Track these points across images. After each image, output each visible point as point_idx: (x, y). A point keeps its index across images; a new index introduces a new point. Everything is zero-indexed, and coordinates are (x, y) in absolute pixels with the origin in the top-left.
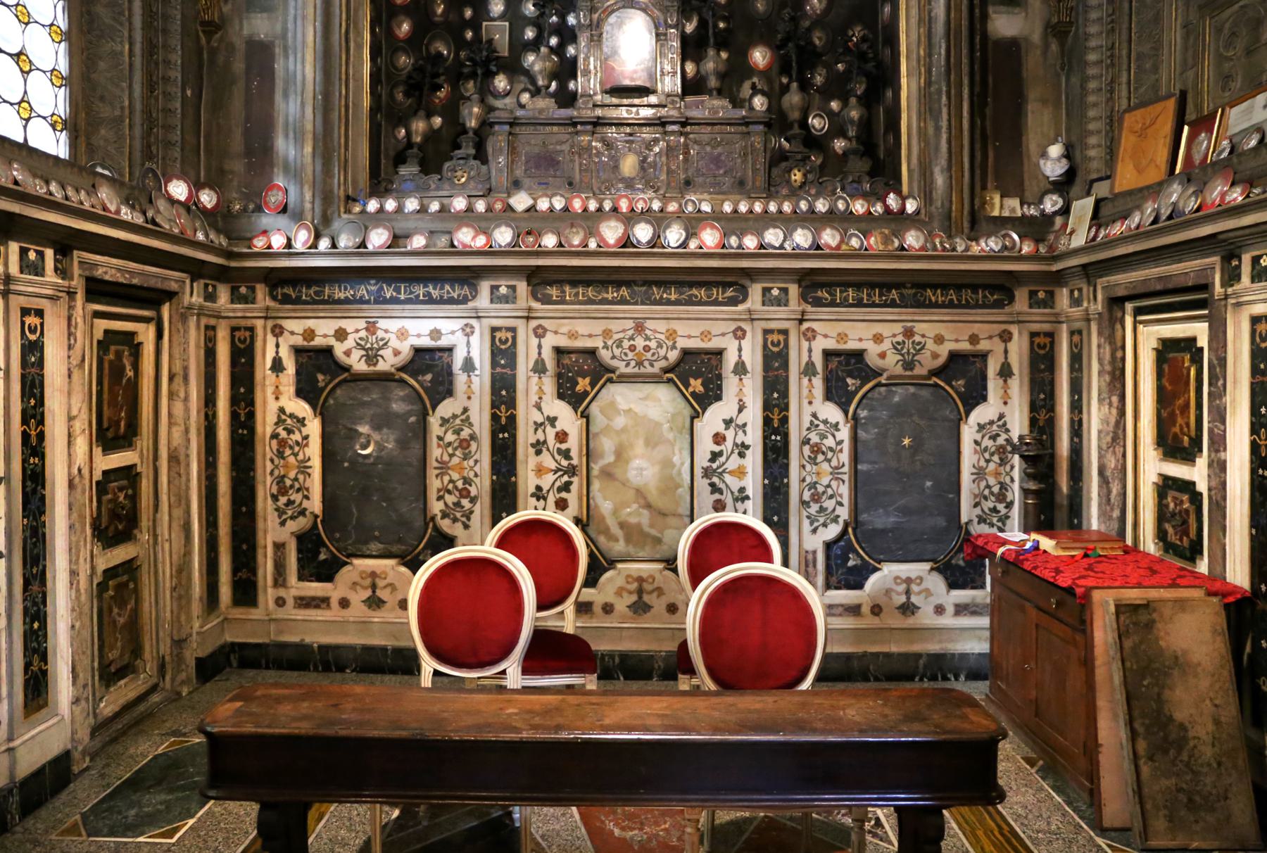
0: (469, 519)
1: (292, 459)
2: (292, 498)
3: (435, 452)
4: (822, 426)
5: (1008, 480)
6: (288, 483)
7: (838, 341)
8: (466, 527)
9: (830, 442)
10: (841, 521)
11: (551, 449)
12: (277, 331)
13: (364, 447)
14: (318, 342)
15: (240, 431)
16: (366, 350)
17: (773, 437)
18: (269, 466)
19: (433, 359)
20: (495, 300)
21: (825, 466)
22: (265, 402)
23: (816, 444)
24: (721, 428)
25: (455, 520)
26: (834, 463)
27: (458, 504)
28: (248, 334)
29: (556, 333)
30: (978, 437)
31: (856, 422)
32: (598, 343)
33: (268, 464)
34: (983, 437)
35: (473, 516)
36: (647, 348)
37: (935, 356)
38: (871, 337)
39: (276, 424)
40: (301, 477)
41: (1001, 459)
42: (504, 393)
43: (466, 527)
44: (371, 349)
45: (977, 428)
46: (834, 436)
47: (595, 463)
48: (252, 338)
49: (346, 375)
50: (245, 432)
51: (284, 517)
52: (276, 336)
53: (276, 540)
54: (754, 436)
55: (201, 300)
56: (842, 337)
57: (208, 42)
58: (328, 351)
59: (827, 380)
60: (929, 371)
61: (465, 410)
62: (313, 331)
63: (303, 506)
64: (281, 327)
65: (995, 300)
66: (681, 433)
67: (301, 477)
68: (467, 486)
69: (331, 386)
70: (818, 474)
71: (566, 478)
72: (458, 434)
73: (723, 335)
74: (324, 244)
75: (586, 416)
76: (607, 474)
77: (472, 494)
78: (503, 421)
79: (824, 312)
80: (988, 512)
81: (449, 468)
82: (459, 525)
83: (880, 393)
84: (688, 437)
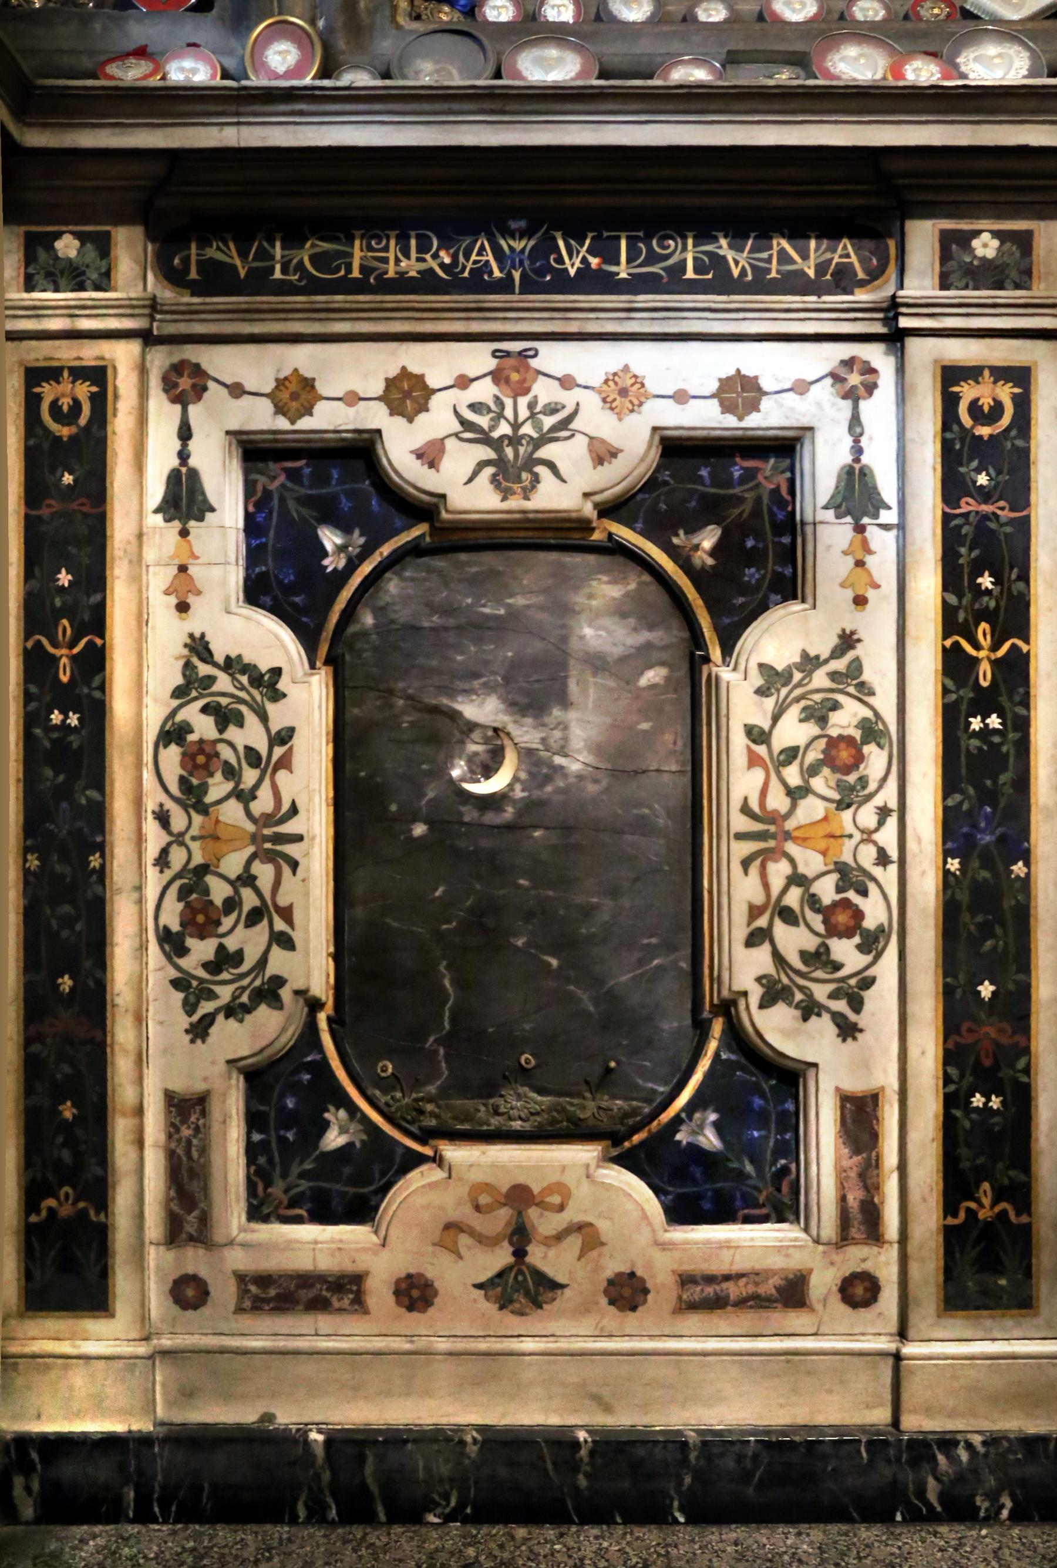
0: (857, 1004)
1: (232, 812)
2: (232, 944)
6: (219, 891)
12: (185, 383)
13: (488, 771)
15: (56, 717)
16: (496, 444)
18: (155, 838)
19: (722, 480)
20: (953, 278)
22: (142, 620)
25: (809, 1010)
28: (83, 390)
33: (151, 827)
35: (870, 996)
39: (179, 693)
40: (264, 873)
42: (986, 581)
43: (847, 1030)
44: (514, 440)
48: (101, 403)
49: (420, 530)
50: (73, 720)
51: (206, 1007)
52: (181, 399)
53: (178, 1086)
62: (308, 384)
63: (271, 970)
64: (198, 371)
67: (264, 873)
68: (851, 895)
69: (366, 568)
72: (822, 721)
77: (870, 923)
78: (985, 675)
81: (788, 836)
82: (824, 1025)
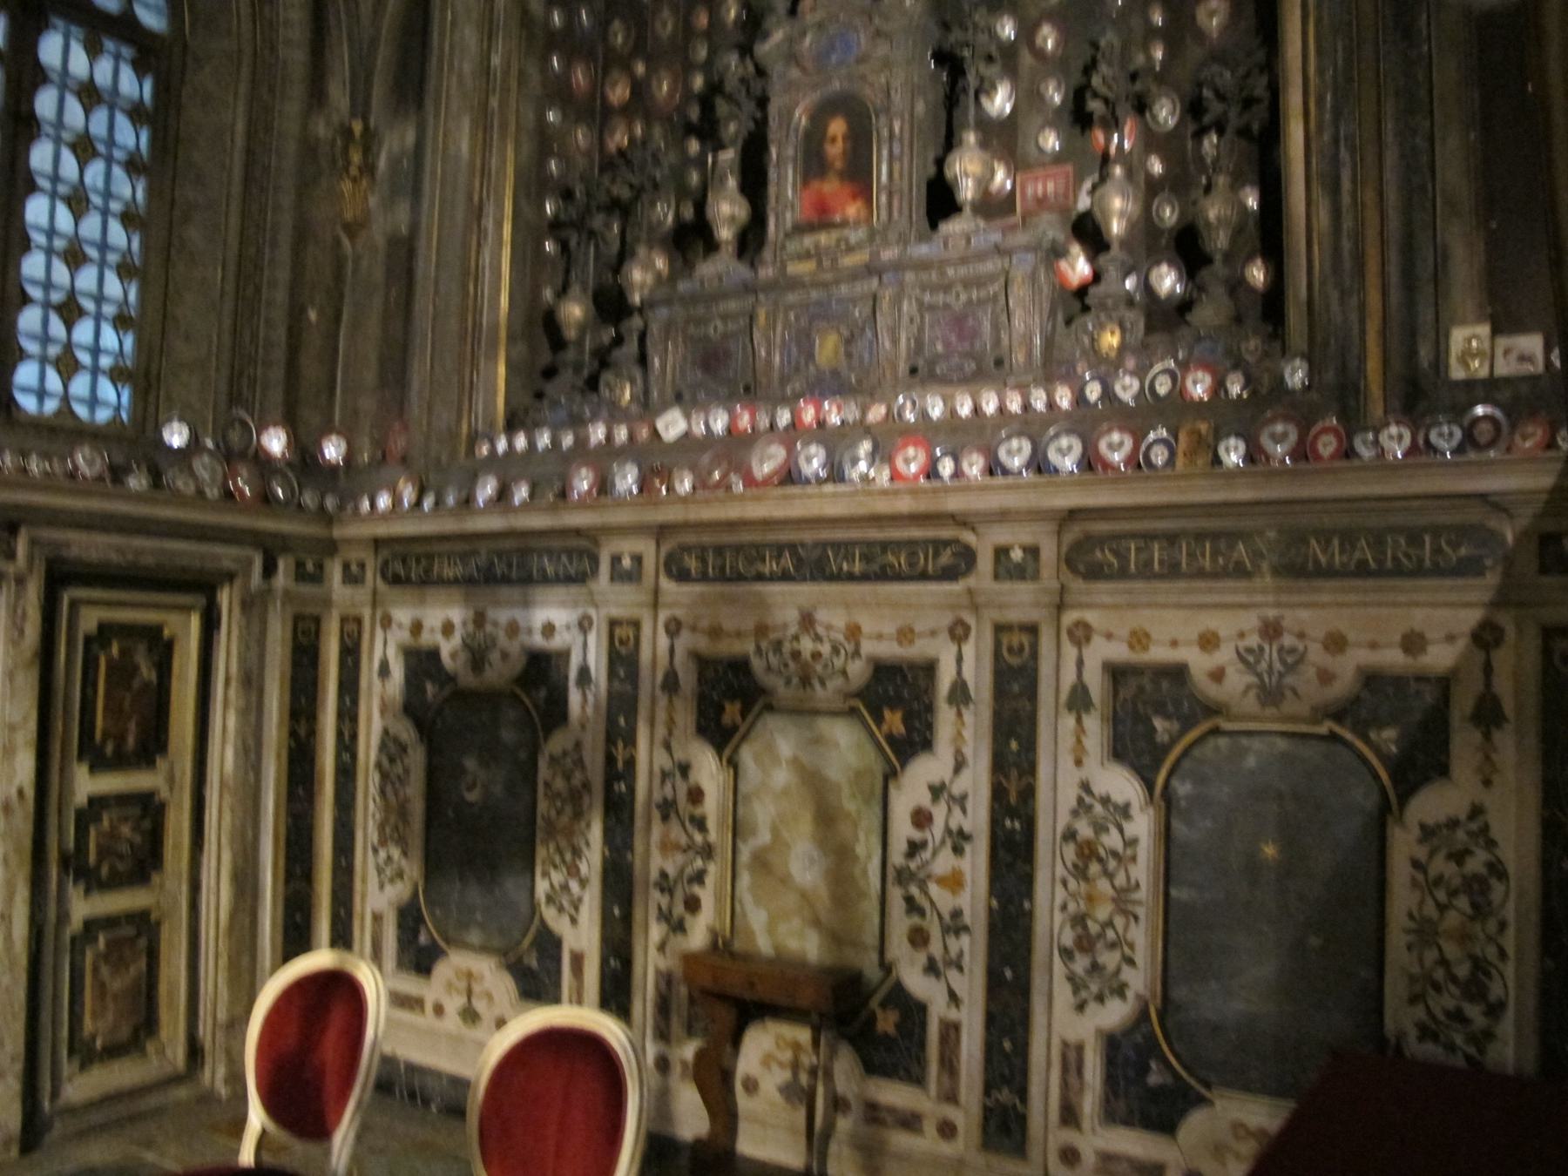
3: (543, 806)
4: (1098, 809)
5: (1491, 952)
7: (1131, 647)
8: (574, 921)
9: (1112, 840)
10: (1130, 994)
11: (681, 813)
13: (470, 788)
14: (426, 639)
17: (1008, 823)
21: (1103, 885)
23: (1089, 843)
24: (925, 799)
26: (1120, 880)
27: (565, 887)
29: (694, 629)
30: (1421, 853)
31: (1167, 804)
32: (749, 647)
34: (1432, 854)
36: (816, 656)
37: (1326, 677)
38: (1195, 636)
41: (1474, 905)
43: (574, 921)
45: (1416, 831)
46: (1121, 831)
47: (745, 841)
54: (977, 818)
55: (291, 584)
56: (1139, 639)
57: (353, 247)
58: (434, 654)
59: (1115, 721)
60: (1314, 709)
61: (578, 745)
65: (1460, 560)
66: (867, 801)
70: (1090, 899)
71: (699, 863)
73: (933, 633)
74: (428, 503)
75: (733, 764)
76: (761, 862)
79: (1103, 591)
80: (1441, 1017)
82: (566, 920)
83: (1217, 749)
84: (877, 810)
